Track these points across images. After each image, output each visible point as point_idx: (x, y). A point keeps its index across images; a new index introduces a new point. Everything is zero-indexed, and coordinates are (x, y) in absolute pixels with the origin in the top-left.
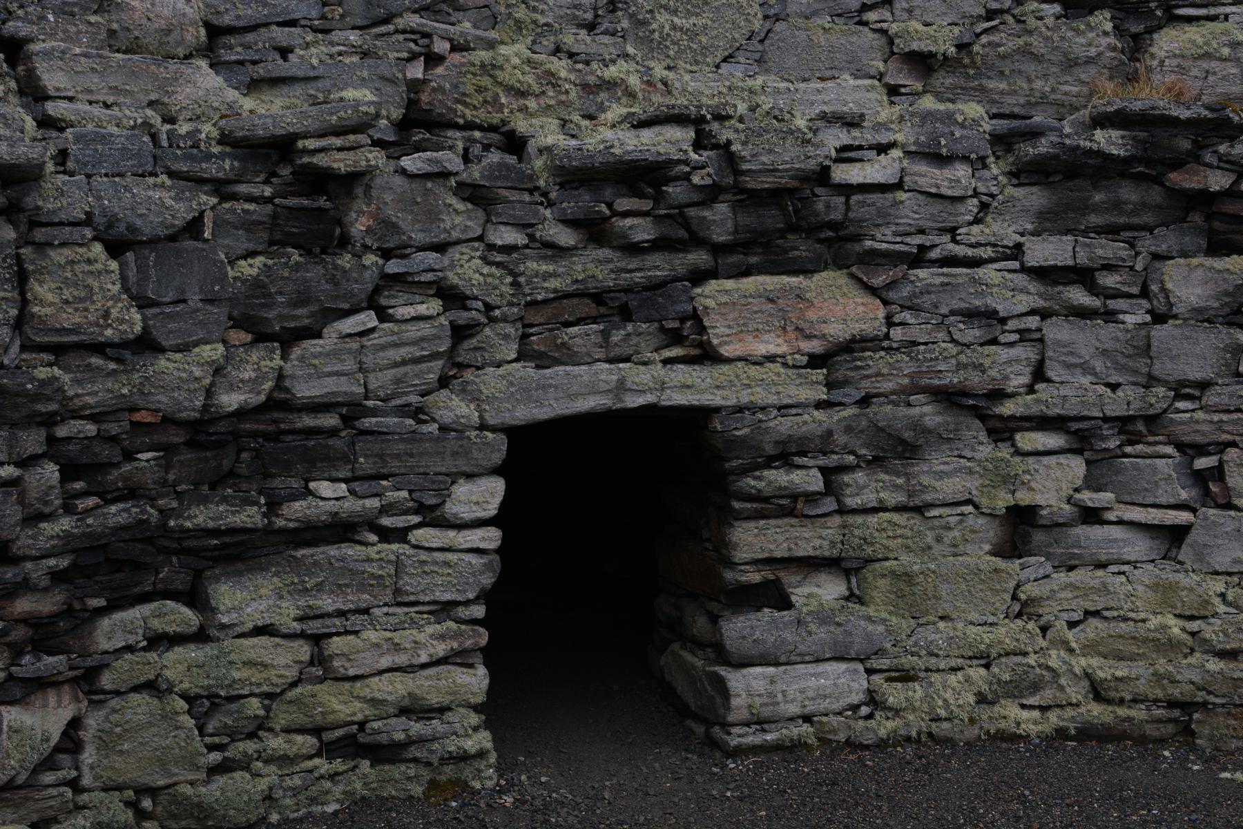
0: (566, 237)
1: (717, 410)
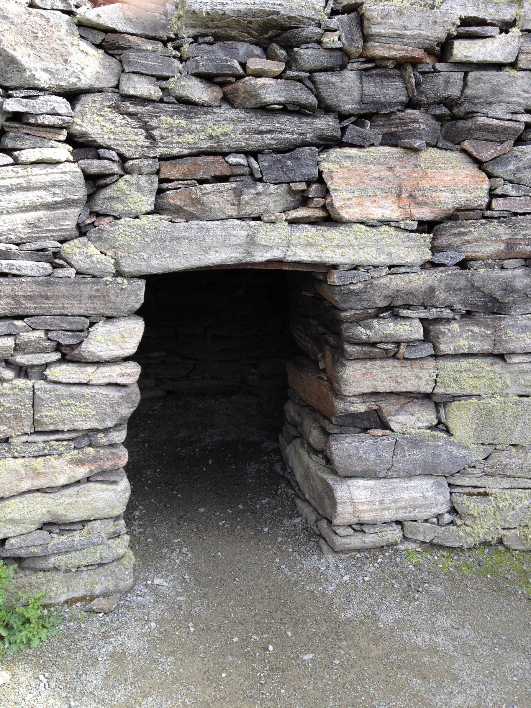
0: (198, 91)
1: (335, 267)
